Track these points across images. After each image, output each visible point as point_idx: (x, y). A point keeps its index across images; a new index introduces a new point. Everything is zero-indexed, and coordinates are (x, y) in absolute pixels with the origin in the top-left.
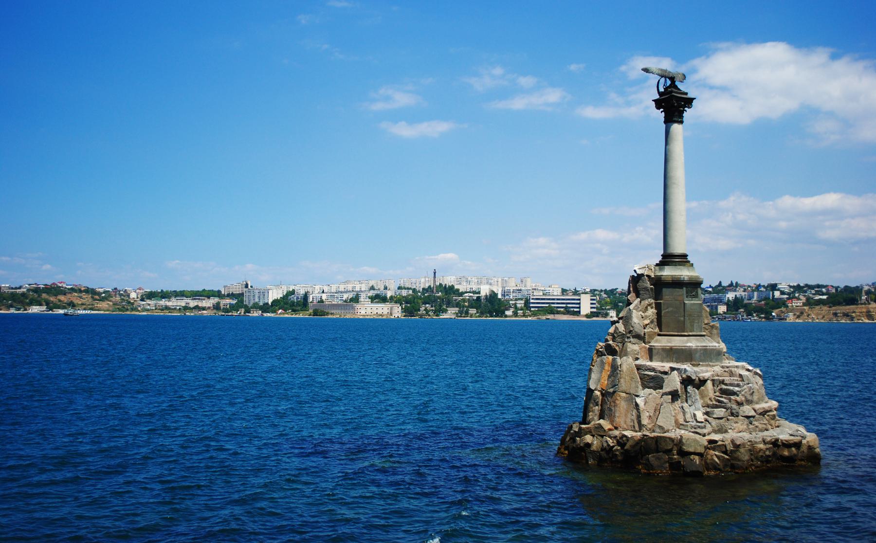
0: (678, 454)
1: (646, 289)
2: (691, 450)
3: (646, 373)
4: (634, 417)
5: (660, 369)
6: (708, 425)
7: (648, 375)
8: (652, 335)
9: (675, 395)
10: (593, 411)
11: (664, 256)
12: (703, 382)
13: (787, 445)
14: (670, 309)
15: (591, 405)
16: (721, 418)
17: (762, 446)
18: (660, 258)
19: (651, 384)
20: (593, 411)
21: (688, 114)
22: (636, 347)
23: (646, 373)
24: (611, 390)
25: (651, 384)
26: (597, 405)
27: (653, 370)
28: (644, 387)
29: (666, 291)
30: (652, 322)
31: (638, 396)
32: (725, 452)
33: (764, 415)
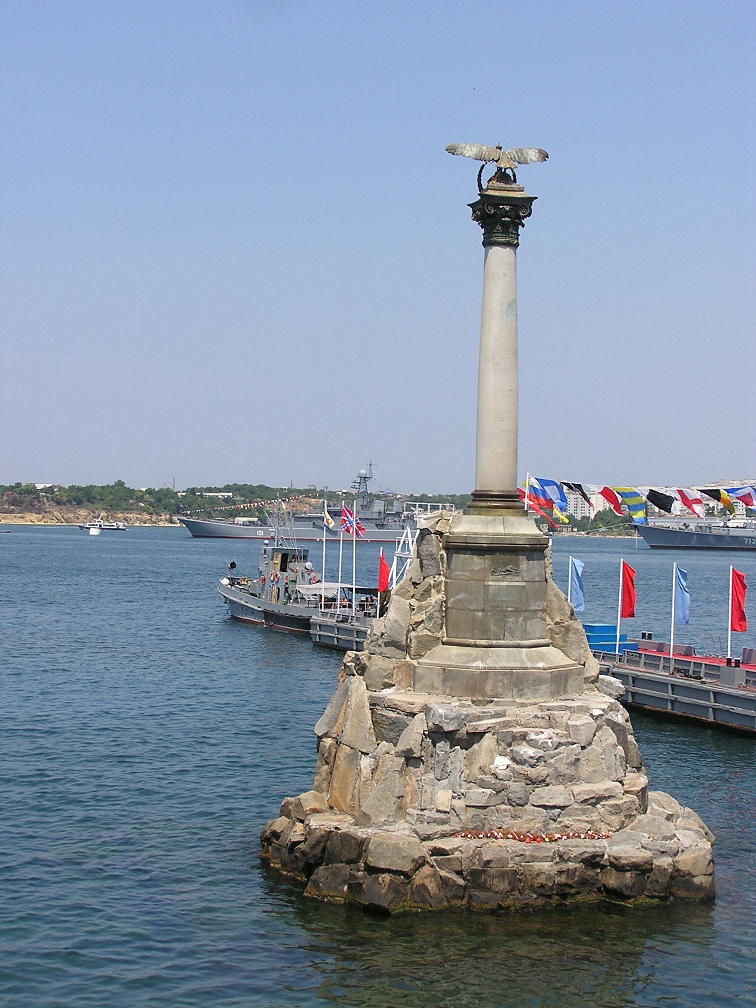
2: (382, 865)
5: (405, 707)
6: (454, 819)
7: (387, 717)
8: (427, 644)
9: (410, 759)
12: (476, 736)
13: (618, 867)
14: (461, 596)
16: (484, 807)
17: (545, 866)
22: (389, 664)
26: (327, 763)
28: (380, 737)
29: (460, 559)
30: (430, 618)
32: (459, 873)
33: (594, 805)
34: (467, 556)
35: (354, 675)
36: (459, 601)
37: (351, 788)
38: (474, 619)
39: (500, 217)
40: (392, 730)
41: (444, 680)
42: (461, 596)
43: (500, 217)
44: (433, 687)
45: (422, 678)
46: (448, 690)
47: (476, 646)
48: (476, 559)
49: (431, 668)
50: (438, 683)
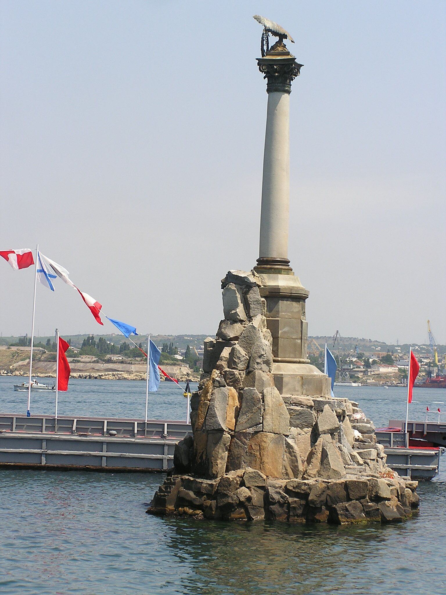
0: (372, 500)
1: (257, 301)
3: (292, 407)
4: (287, 463)
5: (305, 402)
10: (222, 458)
11: (261, 261)
15: (220, 451)
18: (255, 264)
19: (298, 422)
20: (222, 458)
21: (296, 83)
23: (292, 407)
24: (251, 430)
25: (298, 422)
27: (299, 404)
28: (291, 425)
31: (287, 436)
34: (288, 302)
35: (225, 386)
36: (285, 332)
37: (280, 460)
38: (295, 344)
39: (279, 72)
40: (298, 419)
41: (303, 385)
42: (286, 329)
43: (279, 72)
44: (295, 390)
45: (287, 384)
46: (304, 392)
47: (300, 362)
48: (295, 304)
49: (293, 376)
50: (298, 387)
